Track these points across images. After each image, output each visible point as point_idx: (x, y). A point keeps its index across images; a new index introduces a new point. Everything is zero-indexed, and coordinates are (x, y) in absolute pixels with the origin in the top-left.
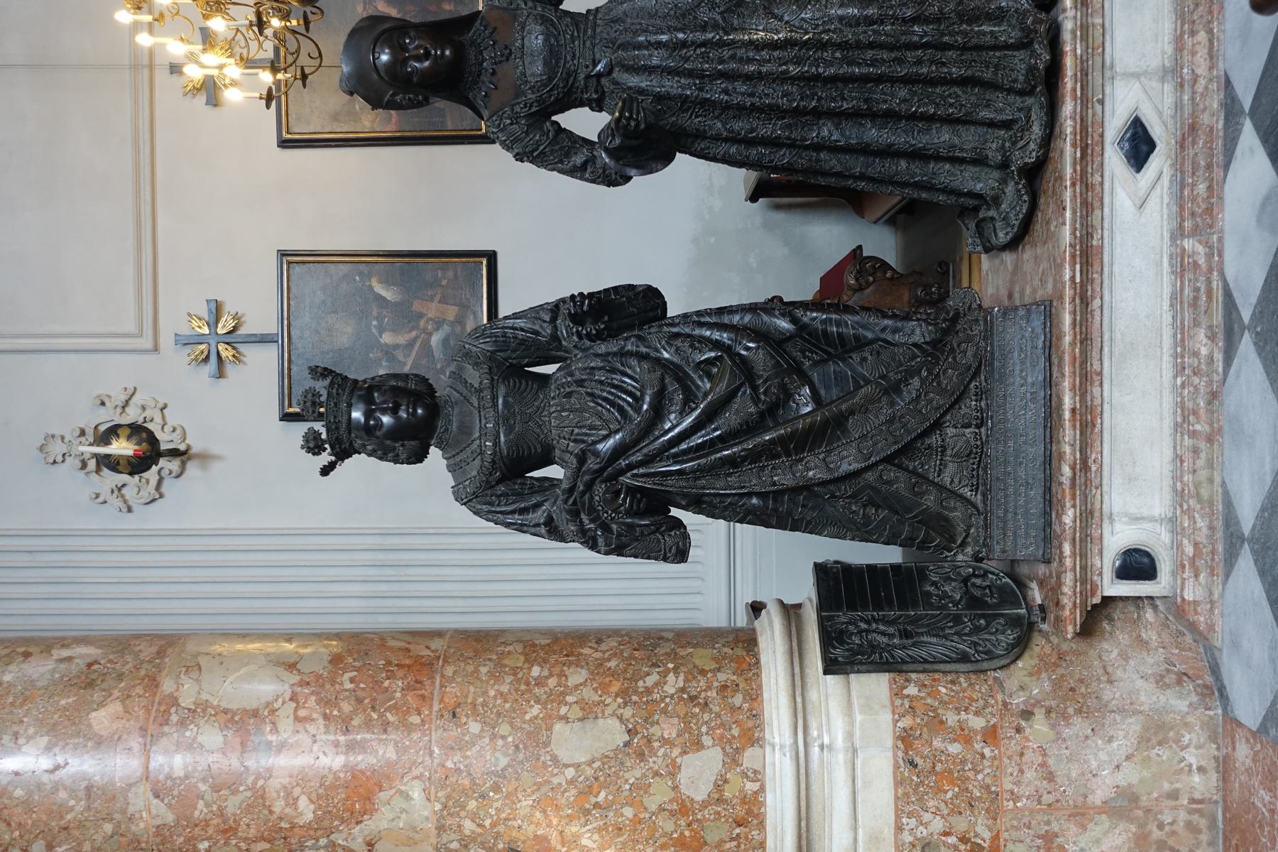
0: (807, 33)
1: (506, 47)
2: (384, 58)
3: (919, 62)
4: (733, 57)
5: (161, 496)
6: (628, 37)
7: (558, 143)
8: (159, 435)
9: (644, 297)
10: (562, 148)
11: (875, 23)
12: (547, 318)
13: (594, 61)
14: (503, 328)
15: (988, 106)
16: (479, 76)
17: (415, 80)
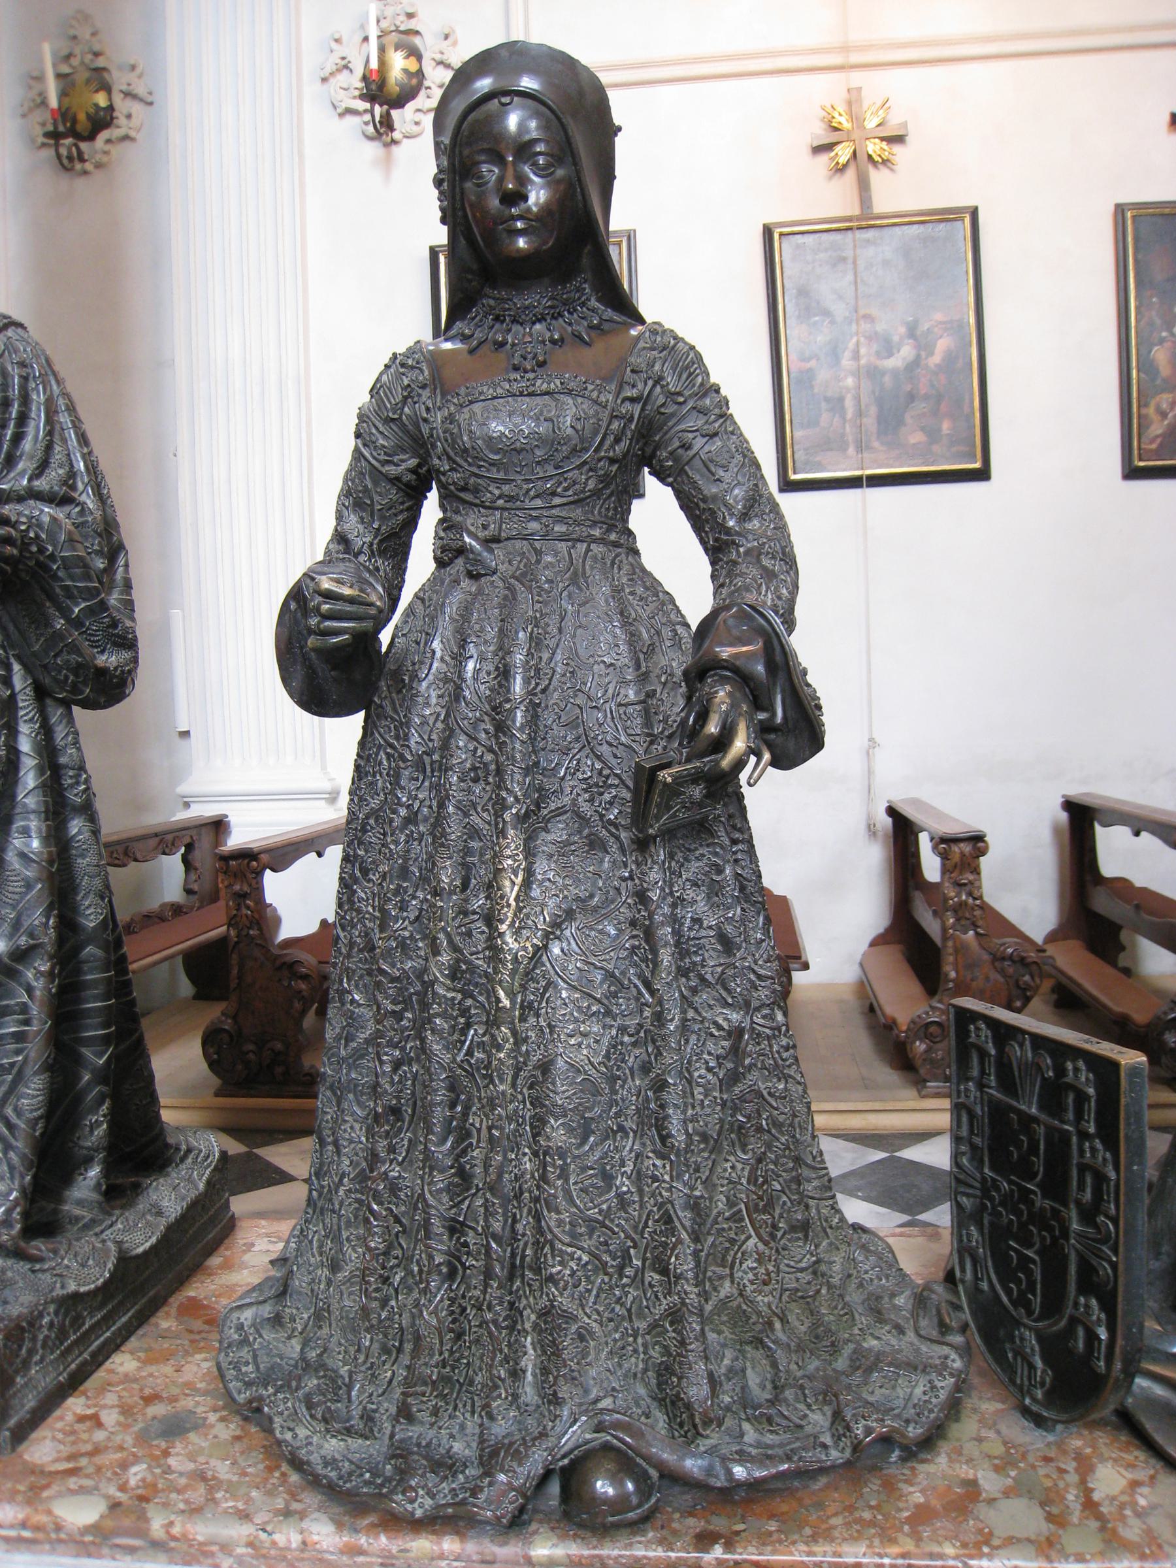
0: (511, 995)
1: (542, 364)
2: (513, 121)
3: (455, 1228)
4: (474, 833)
5: (341, 115)
6: (526, 603)
7: (376, 483)
8: (411, 106)
9: (79, 665)
10: (366, 490)
11: (534, 1136)
12: (42, 484)
13: (496, 540)
14: (25, 400)
15: (385, 1350)
16: (497, 319)
17: (468, 185)
